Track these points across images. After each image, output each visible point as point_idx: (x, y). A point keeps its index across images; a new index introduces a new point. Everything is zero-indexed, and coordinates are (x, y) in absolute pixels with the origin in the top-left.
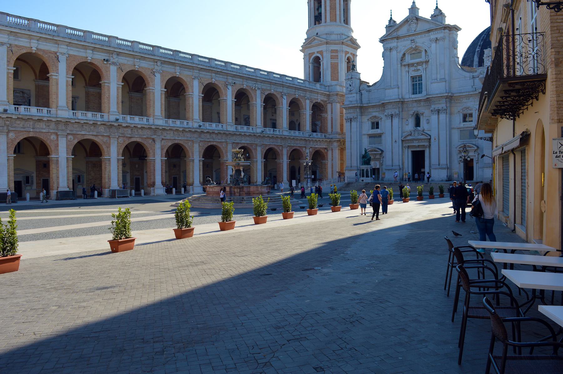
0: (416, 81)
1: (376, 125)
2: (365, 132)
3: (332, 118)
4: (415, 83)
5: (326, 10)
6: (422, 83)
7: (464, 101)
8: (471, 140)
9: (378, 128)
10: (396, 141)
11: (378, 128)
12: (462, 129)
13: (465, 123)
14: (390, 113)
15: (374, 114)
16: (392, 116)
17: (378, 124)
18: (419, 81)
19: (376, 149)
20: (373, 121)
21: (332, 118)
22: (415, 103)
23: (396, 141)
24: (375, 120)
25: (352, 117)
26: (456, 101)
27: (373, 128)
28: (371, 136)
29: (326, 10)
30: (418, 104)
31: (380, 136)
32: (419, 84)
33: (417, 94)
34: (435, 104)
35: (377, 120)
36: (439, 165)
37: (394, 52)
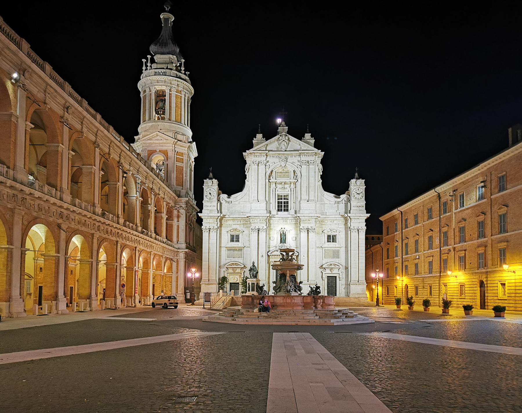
0: (281, 199)
1: (235, 238)
2: (223, 245)
3: (178, 226)
4: (280, 201)
5: (170, 107)
6: (287, 202)
7: (328, 223)
8: (334, 259)
9: (238, 241)
10: (262, 256)
11: (238, 241)
12: (326, 249)
13: (329, 243)
14: (257, 227)
15: (235, 227)
16: (258, 230)
17: (238, 237)
18: (285, 199)
19: (238, 263)
20: (233, 233)
21: (178, 226)
22: (281, 220)
23: (262, 256)
24: (235, 233)
25: (212, 228)
26: (321, 223)
27: (232, 240)
28: (229, 249)
29: (170, 107)
30: (284, 222)
31: (240, 249)
32: (284, 202)
33: (282, 211)
34: (305, 223)
35: (237, 233)
36: (308, 281)
37: (262, 167)
